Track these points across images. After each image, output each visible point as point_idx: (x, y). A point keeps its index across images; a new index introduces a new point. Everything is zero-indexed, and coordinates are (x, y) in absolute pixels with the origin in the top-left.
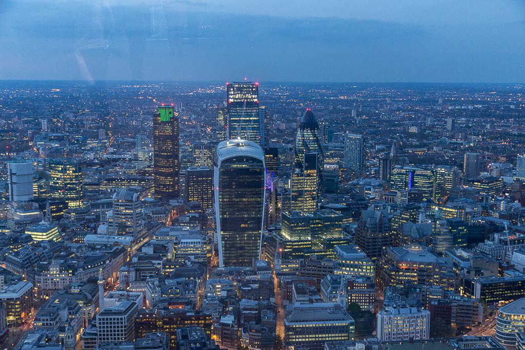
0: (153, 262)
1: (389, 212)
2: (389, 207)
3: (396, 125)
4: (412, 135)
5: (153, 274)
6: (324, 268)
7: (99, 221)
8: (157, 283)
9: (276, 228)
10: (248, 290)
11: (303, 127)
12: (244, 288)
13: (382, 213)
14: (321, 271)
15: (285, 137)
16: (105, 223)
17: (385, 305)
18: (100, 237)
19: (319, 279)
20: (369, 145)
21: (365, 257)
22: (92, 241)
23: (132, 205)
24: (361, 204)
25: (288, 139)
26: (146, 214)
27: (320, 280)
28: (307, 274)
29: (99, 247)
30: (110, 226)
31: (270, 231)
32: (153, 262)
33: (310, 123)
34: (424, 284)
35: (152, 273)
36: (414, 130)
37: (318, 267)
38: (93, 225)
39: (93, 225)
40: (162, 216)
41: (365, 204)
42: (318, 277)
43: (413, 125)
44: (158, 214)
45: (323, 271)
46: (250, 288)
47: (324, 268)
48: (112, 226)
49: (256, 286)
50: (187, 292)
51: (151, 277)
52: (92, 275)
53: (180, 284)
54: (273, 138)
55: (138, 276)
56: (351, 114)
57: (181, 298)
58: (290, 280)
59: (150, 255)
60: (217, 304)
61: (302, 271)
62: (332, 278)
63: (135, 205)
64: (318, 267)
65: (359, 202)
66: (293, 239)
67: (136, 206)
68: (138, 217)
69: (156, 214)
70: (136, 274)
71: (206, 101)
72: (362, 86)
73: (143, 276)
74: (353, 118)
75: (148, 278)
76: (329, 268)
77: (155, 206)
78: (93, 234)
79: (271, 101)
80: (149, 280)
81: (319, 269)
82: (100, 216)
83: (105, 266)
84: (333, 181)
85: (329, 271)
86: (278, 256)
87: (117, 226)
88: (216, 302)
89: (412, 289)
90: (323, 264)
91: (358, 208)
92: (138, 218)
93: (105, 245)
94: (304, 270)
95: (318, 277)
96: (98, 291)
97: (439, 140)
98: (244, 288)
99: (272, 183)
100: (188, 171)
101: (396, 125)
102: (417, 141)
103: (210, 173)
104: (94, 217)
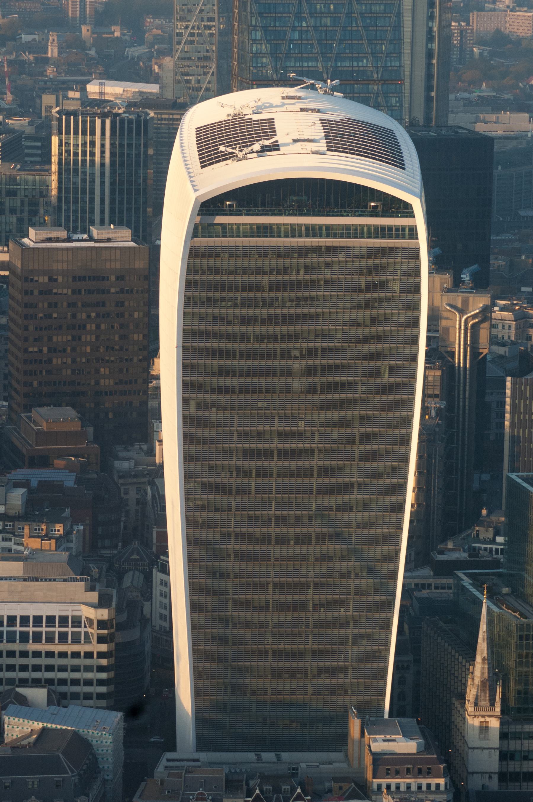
9: (474, 553)
31: (446, 569)
86: (485, 702)
103: (140, 264)
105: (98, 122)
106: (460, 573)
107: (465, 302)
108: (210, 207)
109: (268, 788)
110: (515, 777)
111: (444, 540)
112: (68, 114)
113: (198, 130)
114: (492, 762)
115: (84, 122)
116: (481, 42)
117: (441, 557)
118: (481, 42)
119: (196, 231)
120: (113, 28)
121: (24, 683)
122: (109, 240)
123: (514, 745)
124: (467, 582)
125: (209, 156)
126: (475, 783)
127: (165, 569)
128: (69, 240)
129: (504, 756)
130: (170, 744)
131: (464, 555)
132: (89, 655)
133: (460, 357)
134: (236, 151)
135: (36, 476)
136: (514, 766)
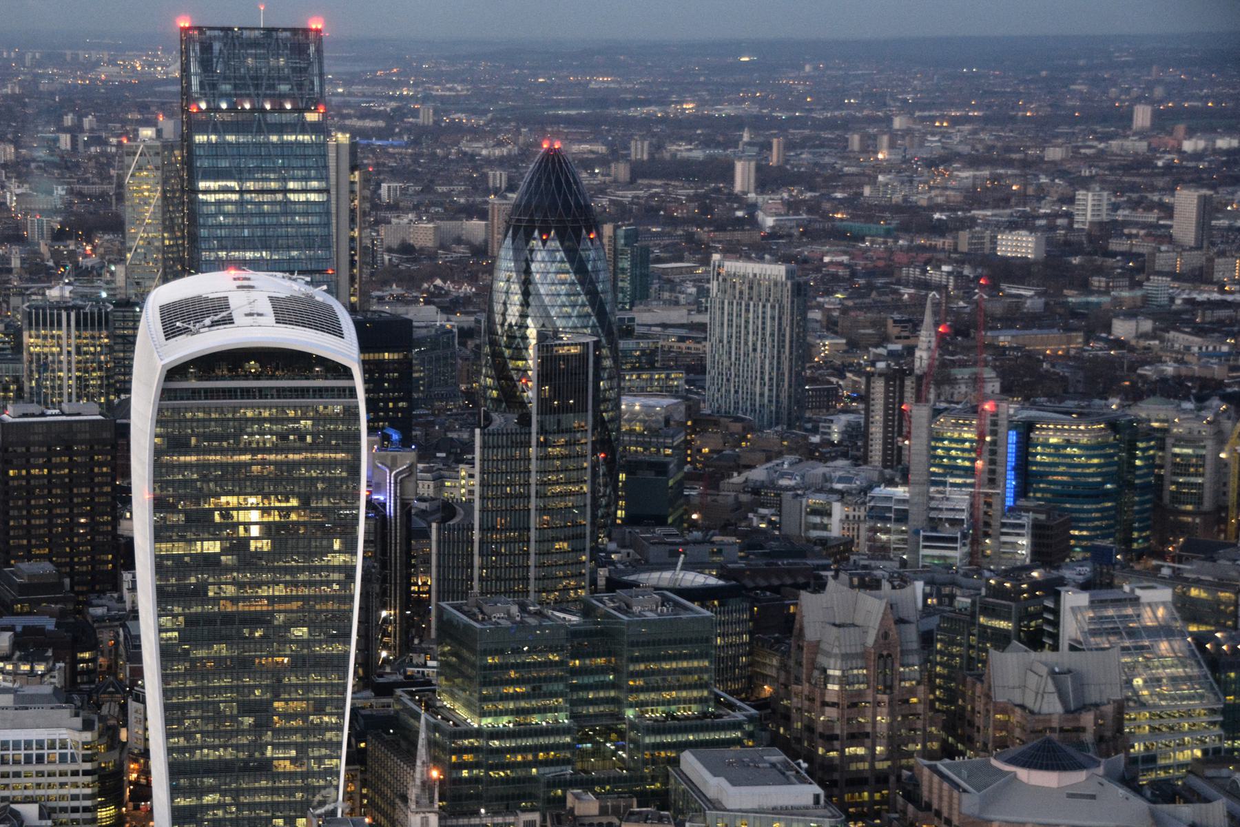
3: (939, 229)
4: (1015, 270)
11: (523, 228)
15: (438, 282)
21: (817, 797)
24: (790, 572)
25: (448, 293)
33: (554, 205)
36: (1019, 245)
56: (730, 179)
65: (782, 563)
66: (487, 722)
71: (68, 120)
72: (778, 57)
74: (739, 199)
79: (368, 123)
86: (425, 801)
91: (776, 589)
99: (390, 478)
101: (939, 229)
102: (1038, 294)
105: (64, 314)
106: (399, 692)
107: (394, 459)
108: (175, 373)
112: (37, 308)
113: (162, 308)
115: (52, 315)
116: (390, 250)
117: (381, 680)
118: (390, 250)
119: (166, 394)
120: (69, 242)
122: (79, 414)
124: (406, 698)
125: (171, 332)
128: (43, 415)
133: (390, 509)
134: (191, 327)
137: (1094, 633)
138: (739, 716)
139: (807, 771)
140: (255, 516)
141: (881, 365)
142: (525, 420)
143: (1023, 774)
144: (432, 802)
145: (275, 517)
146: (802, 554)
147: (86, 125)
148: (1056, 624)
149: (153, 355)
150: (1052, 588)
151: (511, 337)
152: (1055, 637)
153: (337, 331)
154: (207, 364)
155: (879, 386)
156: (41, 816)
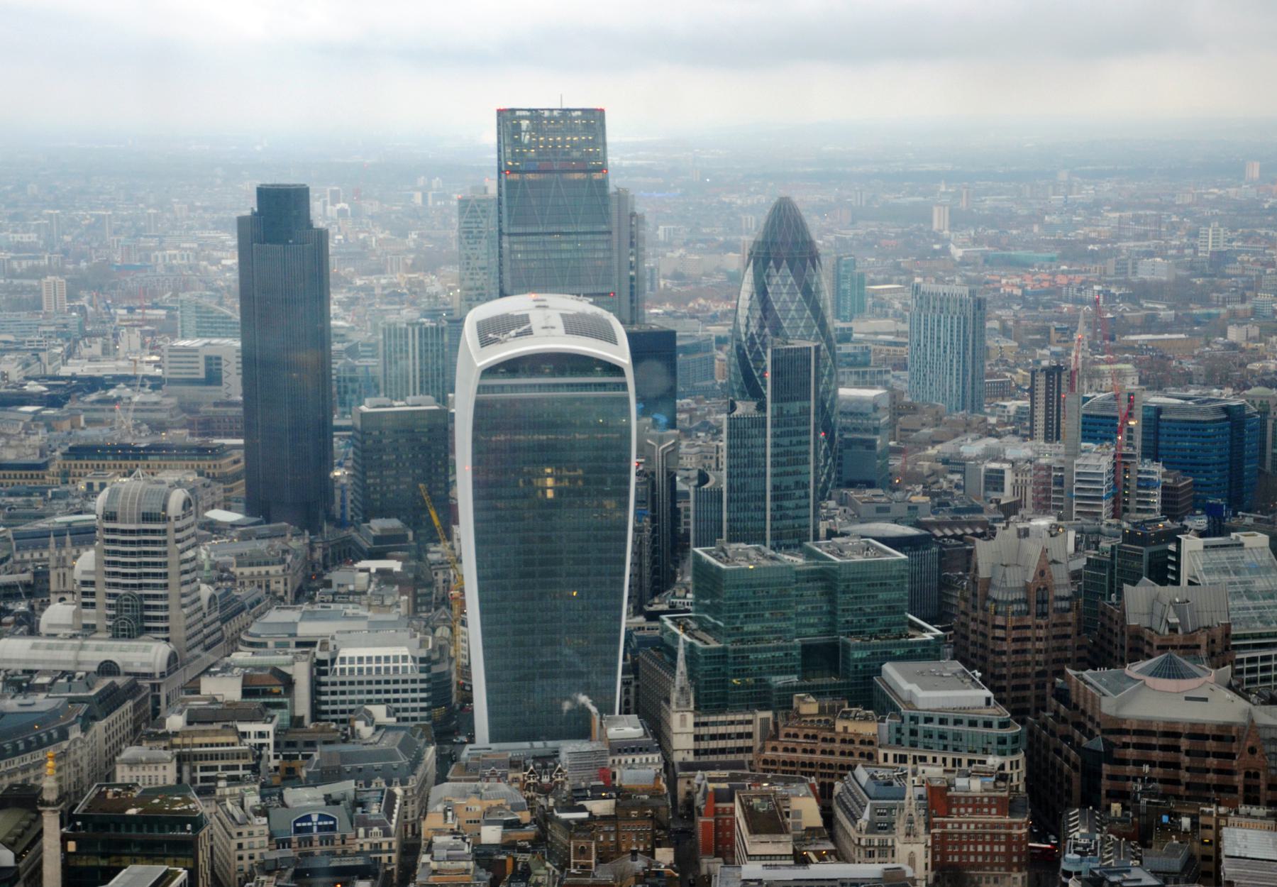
0: (242, 727)
1: (1071, 547)
2: (1072, 535)
5: (240, 772)
6: (843, 741)
7: (47, 592)
8: (253, 800)
9: (673, 606)
10: (581, 822)
12: (565, 816)
13: (1045, 551)
14: (832, 753)
15: (702, 301)
16: (68, 597)
17: (1068, 874)
18: (49, 647)
19: (827, 780)
20: (995, 324)
21: (988, 700)
22: (18, 661)
23: (164, 532)
24: (970, 524)
26: (214, 566)
27: (832, 786)
28: (784, 763)
29: (46, 680)
30: (85, 605)
31: (654, 616)
32: (242, 727)
34: (1209, 801)
35: (236, 768)
37: (824, 740)
38: (22, 607)
39: (22, 607)
40: (272, 569)
41: (984, 524)
42: (822, 775)
43: (1150, 254)
44: (259, 564)
45: (843, 753)
46: (585, 815)
47: (843, 741)
48: (93, 605)
49: (601, 807)
50: (361, 831)
51: (233, 780)
52: (19, 778)
53: (337, 803)
54: (660, 303)
55: (186, 777)
57: (339, 851)
58: (725, 786)
59: (234, 703)
60: (467, 871)
61: (768, 754)
62: (872, 777)
63: (177, 531)
64: (824, 740)
65: (964, 517)
67: (179, 536)
68: (186, 572)
69: (251, 565)
70: (179, 770)
71: (422, 181)
73: (204, 779)
75: (222, 784)
76: (862, 742)
77: (245, 537)
78: (22, 634)
80: (227, 791)
81: (827, 746)
82: (48, 573)
83: (65, 745)
84: (870, 445)
85: (862, 755)
86: (683, 702)
87: (110, 606)
88: (464, 864)
89: (1165, 819)
90: (839, 726)
92: (187, 577)
93: (68, 675)
94: (774, 749)
95: (822, 775)
96: (40, 834)
97: (1248, 306)
98: (565, 816)
100: (363, 415)
103: (440, 421)
104: (27, 577)
106: (664, 617)
109: (538, 764)
110: (706, 752)
111: (652, 598)
114: (690, 744)
116: (665, 277)
117: (651, 609)
121: (370, 702)
123: (703, 730)
124: (668, 623)
125: (485, 342)
126: (677, 758)
127: (464, 623)
129: (697, 738)
130: (471, 740)
131: (666, 607)
132: (414, 681)
135: (374, 565)
136: (703, 745)
137: (1208, 572)
138: (928, 636)
139: (981, 679)
140: (550, 482)
141: (1045, 363)
142: (761, 407)
143: (1150, 681)
144: (688, 703)
145: (566, 483)
146: (980, 510)
147: (435, 185)
148: (1177, 564)
149: (474, 358)
150: (1172, 536)
151: (753, 343)
152: (1177, 574)
153: (611, 338)
154: (512, 367)
155: (1041, 379)
156: (389, 715)
